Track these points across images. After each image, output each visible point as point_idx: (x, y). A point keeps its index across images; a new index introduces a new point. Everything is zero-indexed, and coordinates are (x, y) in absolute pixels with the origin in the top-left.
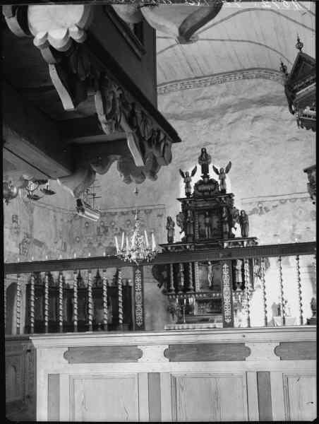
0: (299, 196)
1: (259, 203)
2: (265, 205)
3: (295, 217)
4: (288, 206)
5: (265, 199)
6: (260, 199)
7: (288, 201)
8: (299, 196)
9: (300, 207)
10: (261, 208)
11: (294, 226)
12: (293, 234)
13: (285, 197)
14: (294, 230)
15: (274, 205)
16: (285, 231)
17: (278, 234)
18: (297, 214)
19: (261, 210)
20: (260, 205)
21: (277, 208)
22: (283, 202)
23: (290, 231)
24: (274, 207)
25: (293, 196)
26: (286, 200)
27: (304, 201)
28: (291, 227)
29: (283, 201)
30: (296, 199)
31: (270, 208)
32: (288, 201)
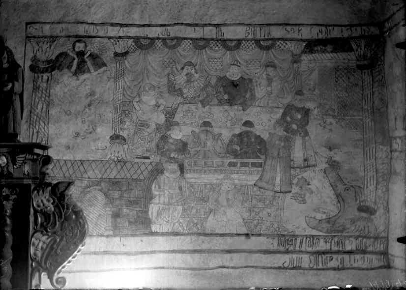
0: (191, 33)
1: (79, 38)
2: (93, 47)
3: (173, 89)
4: (155, 59)
5: (92, 31)
6: (81, 30)
7: (159, 44)
8: (191, 33)
9: (190, 64)
10: (81, 54)
11: (170, 114)
12: (164, 138)
13: (153, 32)
14: (170, 123)
15: (119, 51)
16: (144, 125)
17: (125, 134)
18: (181, 79)
19: (82, 63)
20: (80, 47)
21: (128, 62)
22: (144, 44)
23: (158, 128)
24: (116, 55)
25: (174, 31)
26: (153, 40)
27: (203, 47)
28: (162, 119)
29: (143, 42)
30: (179, 40)
31: (108, 56)
32: (159, 44)
